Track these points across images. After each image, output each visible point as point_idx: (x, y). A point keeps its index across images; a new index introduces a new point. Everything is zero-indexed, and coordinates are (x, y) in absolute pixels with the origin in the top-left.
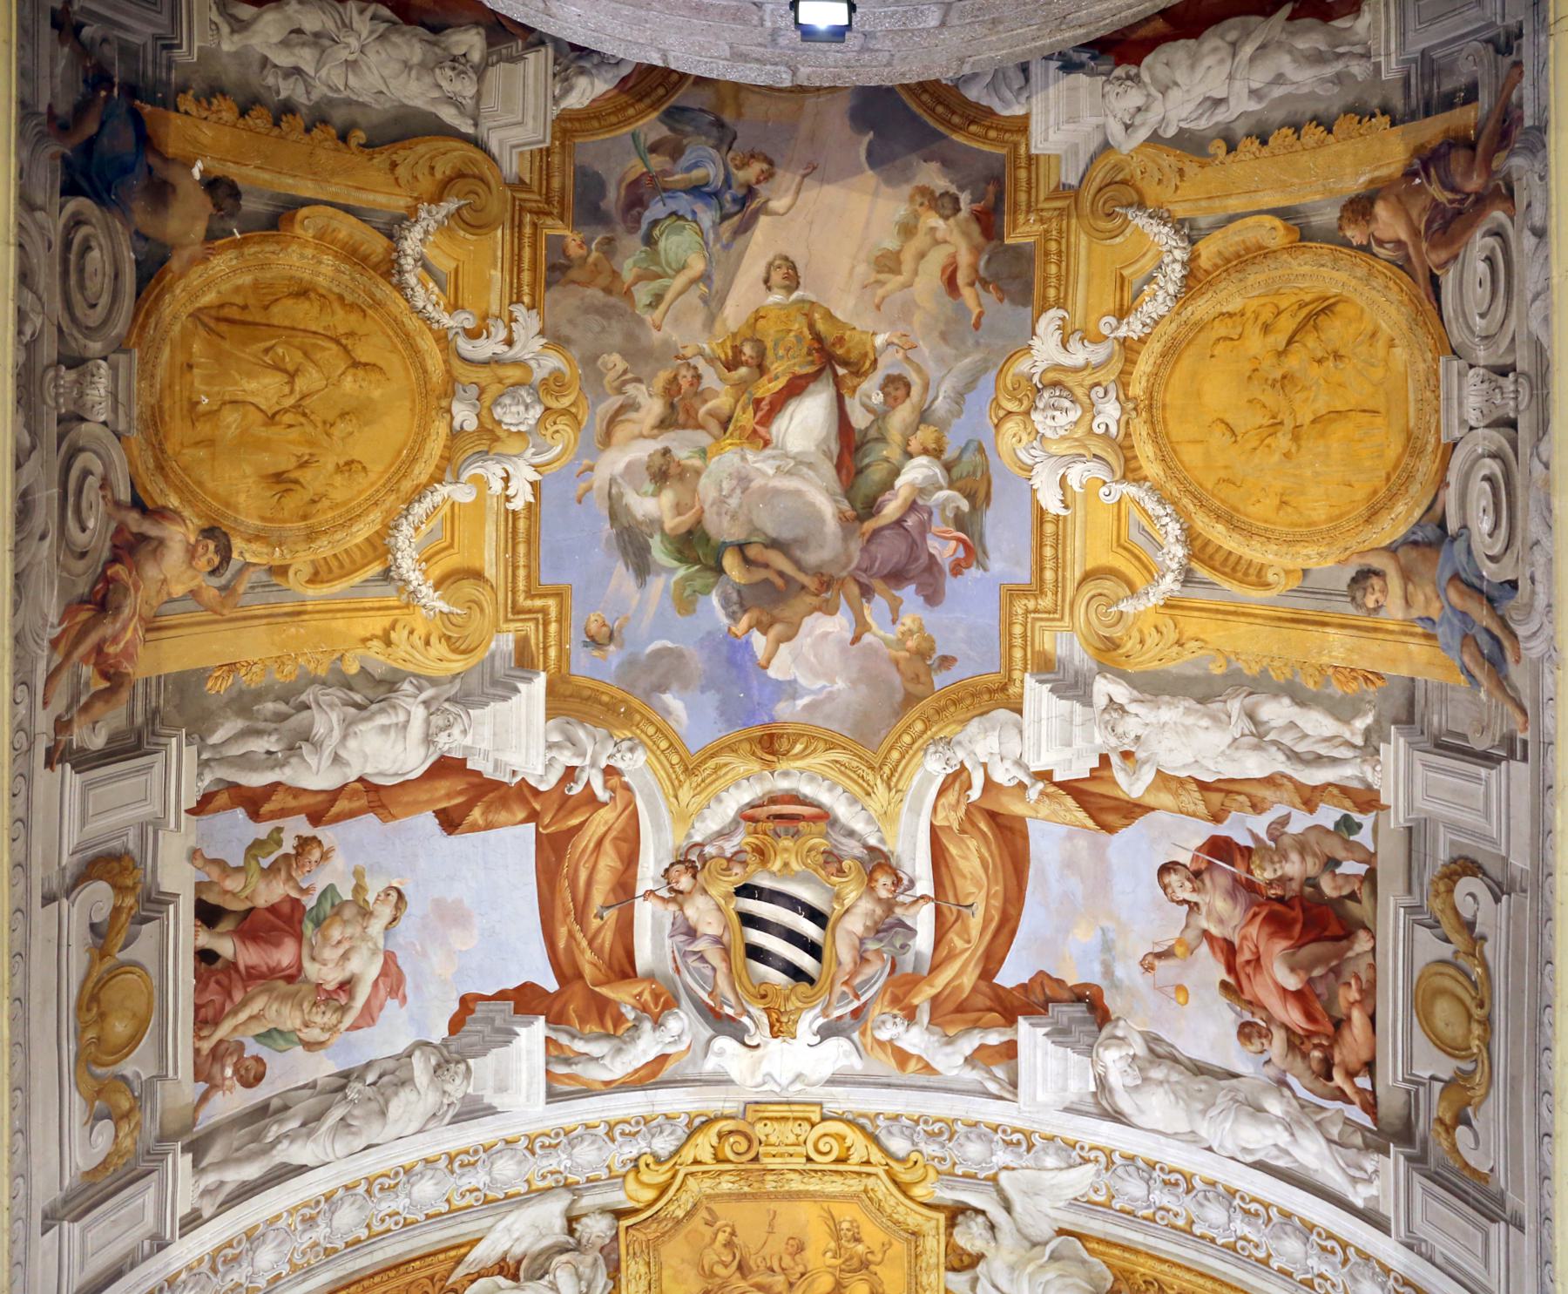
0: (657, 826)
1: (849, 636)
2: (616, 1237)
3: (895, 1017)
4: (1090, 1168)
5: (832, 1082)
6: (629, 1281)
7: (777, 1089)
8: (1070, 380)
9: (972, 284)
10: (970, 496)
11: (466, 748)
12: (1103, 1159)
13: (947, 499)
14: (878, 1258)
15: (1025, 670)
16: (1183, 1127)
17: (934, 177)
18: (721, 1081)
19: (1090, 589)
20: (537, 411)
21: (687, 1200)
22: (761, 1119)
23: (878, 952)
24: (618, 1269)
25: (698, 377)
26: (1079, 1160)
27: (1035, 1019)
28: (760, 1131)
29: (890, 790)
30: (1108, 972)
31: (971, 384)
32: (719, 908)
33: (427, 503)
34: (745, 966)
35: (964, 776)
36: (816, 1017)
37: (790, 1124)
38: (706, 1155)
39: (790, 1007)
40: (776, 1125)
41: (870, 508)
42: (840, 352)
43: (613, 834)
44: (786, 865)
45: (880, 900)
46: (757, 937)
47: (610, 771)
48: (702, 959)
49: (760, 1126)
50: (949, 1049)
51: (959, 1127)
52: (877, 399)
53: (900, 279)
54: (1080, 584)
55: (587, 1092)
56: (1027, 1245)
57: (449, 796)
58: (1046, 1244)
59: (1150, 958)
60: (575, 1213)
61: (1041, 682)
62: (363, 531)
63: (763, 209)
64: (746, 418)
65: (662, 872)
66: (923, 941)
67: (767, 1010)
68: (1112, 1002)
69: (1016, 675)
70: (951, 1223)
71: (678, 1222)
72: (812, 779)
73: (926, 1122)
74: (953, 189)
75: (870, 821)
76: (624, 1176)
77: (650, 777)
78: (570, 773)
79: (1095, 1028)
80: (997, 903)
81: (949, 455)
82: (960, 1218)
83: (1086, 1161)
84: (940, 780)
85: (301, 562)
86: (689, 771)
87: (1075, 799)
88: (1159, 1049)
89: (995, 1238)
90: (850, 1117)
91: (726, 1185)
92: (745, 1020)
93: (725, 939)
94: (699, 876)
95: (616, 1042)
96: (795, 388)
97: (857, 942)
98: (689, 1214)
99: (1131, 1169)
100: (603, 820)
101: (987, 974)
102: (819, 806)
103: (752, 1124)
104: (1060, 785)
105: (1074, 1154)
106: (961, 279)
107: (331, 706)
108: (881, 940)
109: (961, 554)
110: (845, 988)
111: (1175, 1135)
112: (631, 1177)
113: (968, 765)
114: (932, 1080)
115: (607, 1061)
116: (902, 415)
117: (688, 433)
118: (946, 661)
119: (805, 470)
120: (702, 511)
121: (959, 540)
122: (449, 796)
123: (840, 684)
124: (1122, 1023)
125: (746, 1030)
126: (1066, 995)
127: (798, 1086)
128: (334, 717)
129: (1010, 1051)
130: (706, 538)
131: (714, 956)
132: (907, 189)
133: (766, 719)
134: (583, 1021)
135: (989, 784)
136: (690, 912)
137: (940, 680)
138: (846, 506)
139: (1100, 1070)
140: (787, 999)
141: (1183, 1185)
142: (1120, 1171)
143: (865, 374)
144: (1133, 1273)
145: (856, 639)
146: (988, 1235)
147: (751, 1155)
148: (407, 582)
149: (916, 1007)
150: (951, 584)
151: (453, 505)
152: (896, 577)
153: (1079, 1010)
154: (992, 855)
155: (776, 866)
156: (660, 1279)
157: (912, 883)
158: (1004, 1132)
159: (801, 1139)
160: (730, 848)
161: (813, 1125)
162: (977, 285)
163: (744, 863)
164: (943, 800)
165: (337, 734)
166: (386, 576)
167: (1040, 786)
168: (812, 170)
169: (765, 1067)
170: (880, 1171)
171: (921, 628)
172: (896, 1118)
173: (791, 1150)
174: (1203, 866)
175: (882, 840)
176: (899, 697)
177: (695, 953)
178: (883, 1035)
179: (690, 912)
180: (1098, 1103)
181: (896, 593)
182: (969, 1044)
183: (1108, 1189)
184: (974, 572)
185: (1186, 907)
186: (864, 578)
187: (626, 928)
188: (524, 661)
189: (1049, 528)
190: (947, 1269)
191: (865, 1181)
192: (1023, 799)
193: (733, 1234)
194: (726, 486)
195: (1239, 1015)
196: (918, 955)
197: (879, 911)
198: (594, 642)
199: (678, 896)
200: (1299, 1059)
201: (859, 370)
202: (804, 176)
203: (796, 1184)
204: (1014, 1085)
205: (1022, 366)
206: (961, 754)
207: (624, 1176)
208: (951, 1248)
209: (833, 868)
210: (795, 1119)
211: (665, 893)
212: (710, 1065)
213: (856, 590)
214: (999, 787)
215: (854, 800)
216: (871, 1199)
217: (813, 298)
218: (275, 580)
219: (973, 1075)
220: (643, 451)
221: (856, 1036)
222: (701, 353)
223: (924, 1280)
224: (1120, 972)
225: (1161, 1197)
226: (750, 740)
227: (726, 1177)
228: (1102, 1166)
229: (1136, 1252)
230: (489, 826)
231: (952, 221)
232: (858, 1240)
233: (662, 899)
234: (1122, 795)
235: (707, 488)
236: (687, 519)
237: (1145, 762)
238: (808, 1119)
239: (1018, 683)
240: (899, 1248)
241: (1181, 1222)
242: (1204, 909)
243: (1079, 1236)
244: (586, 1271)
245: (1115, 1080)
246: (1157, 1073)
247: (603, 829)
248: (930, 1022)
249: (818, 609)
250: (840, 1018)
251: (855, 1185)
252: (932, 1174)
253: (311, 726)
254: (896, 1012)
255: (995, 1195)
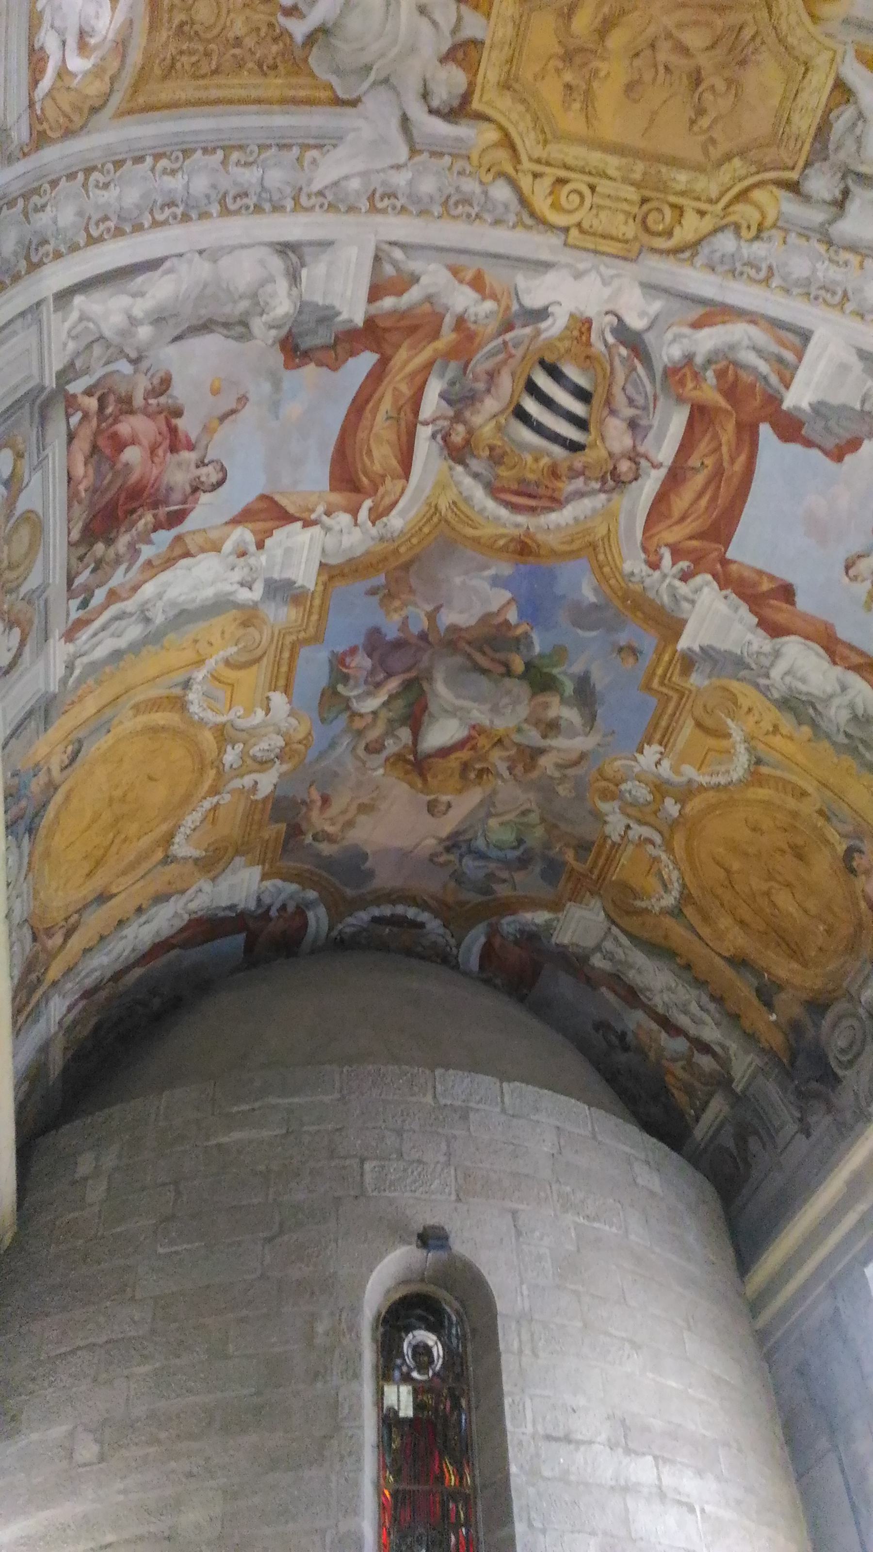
0: (632, 515)
1: (443, 610)
2: (808, 164)
3: (475, 322)
4: (316, 186)
5: (546, 266)
6: (814, 110)
7: (602, 268)
8: (256, 766)
9: (312, 801)
10: (335, 693)
11: (754, 633)
12: (304, 201)
13: (352, 690)
14: (553, 63)
15: (313, 593)
16: (225, 262)
17: (326, 849)
18: (650, 288)
19: (259, 652)
20: (623, 787)
21: (725, 174)
22: (626, 242)
23: (476, 379)
24: (819, 128)
25: (510, 769)
26: (327, 193)
27: (348, 327)
28: (630, 230)
29: (436, 507)
30: (277, 385)
31: (322, 755)
32: (603, 439)
33: (715, 780)
34: (596, 386)
35: (372, 517)
36: (546, 330)
37: (600, 230)
38: (691, 220)
39: (567, 343)
40: (614, 233)
41: (408, 685)
42: (409, 767)
43: (669, 522)
44: (536, 460)
45: (465, 423)
46: (577, 408)
47: (655, 565)
48: (631, 402)
49: (630, 235)
50: (431, 290)
51: (437, 210)
52: (389, 742)
53: (360, 801)
54: (265, 653)
55: (775, 325)
56: (393, 80)
57: (780, 610)
58: (374, 84)
59: (240, 408)
60: (834, 210)
61: (302, 587)
62: (763, 793)
63: (441, 841)
64: (482, 741)
65: (640, 481)
66: (434, 388)
67: (589, 344)
68: (277, 358)
69: (320, 588)
70: (466, 98)
71: (742, 153)
72: (497, 519)
73: (469, 216)
74: (316, 844)
75: (458, 484)
76: (774, 226)
77: (625, 551)
78: (685, 577)
79: (294, 330)
80: (365, 423)
81: (345, 716)
82: (456, 103)
83: (321, 193)
84: (394, 512)
85: (807, 808)
86: (593, 546)
87: (286, 512)
88: (240, 329)
89: (425, 81)
90: (541, 227)
91: (682, 178)
92: (611, 340)
93: (606, 412)
94: (612, 467)
95: (731, 356)
96: (444, 752)
97: (493, 390)
98: (728, 157)
99: (276, 197)
100: (674, 535)
101: (384, 362)
102: (496, 499)
103: (636, 238)
104: (297, 519)
105: (330, 197)
106: (319, 803)
107: (830, 721)
108: (471, 390)
109: (348, 660)
110: (513, 351)
111: (232, 249)
112: (769, 221)
113: (370, 524)
114: (452, 259)
115: (746, 342)
116: (374, 734)
117: (525, 742)
118: (373, 592)
119: (449, 709)
120: (530, 700)
121: (348, 667)
122: (780, 610)
123: (458, 580)
124: (270, 342)
125: (614, 331)
126: (319, 355)
127: (581, 266)
128: (832, 711)
129: (375, 293)
130: (532, 685)
131: (620, 400)
132: (345, 843)
133: (521, 566)
134: (753, 386)
135: (354, 512)
136: (628, 442)
137: (380, 579)
138: (425, 686)
139: (295, 291)
140: (568, 351)
141: (229, 200)
142: (288, 190)
143: (394, 754)
144: (288, 74)
145: (438, 609)
146: (432, 86)
147: (646, 207)
148: (747, 749)
149: (453, 331)
150: (360, 641)
151: (699, 770)
152: (399, 645)
153: (306, 343)
154: (362, 460)
155: (545, 461)
156: (784, 98)
157: (434, 436)
158: (394, 208)
159: (594, 211)
160: (579, 483)
161: (579, 225)
162: (308, 801)
163: (570, 468)
164: (393, 498)
165: (836, 702)
166: (759, 762)
167: (313, 516)
168: (404, 855)
169: (607, 292)
170: (526, 165)
171: (388, 613)
172: (497, 222)
173: (607, 202)
174: (191, 498)
175: (451, 468)
176: (414, 569)
177: (637, 407)
178: (489, 305)
179: (628, 442)
180: (300, 258)
181: (401, 635)
182: (414, 295)
183: (302, 167)
184: (340, 649)
185: (206, 461)
186: (422, 644)
187: (686, 446)
188: (688, 663)
189: (282, 682)
190: (482, 43)
191: (544, 155)
192: (329, 504)
193: (693, 122)
194: (508, 711)
195: (171, 396)
196: (442, 376)
197: (467, 414)
198: (634, 652)
199: (634, 457)
200: (123, 394)
201: (399, 758)
202: (411, 852)
203: (612, 163)
204: (377, 259)
205: (285, 767)
206: (374, 531)
207: (774, 226)
208: (472, 68)
209: (498, 451)
210: (594, 234)
211: (644, 463)
212: (656, 306)
213: (431, 638)
214: (346, 510)
215: (468, 500)
216: (543, 131)
217: (421, 795)
218: (828, 813)
219: (414, 265)
220: (559, 742)
221: (515, 307)
222: (504, 780)
223: (510, 31)
224: (267, 387)
225: (249, 176)
226: (538, 555)
227: (680, 187)
228: (305, 190)
229: (284, 101)
230: (760, 573)
231: (319, 829)
232: (568, 87)
233: (647, 458)
234: (250, 525)
235: (523, 711)
236: (541, 699)
237: (231, 554)
238: (582, 231)
239: (320, 583)
240: (528, 72)
241: (235, 156)
242: (193, 466)
243: (338, 102)
244: (850, 145)
245: (282, 285)
246: (244, 305)
247: (675, 528)
248: (442, 317)
249: (461, 629)
250: (524, 326)
251: (556, 151)
252: (475, 156)
253: (849, 721)
254: (473, 327)
255: (415, 133)
